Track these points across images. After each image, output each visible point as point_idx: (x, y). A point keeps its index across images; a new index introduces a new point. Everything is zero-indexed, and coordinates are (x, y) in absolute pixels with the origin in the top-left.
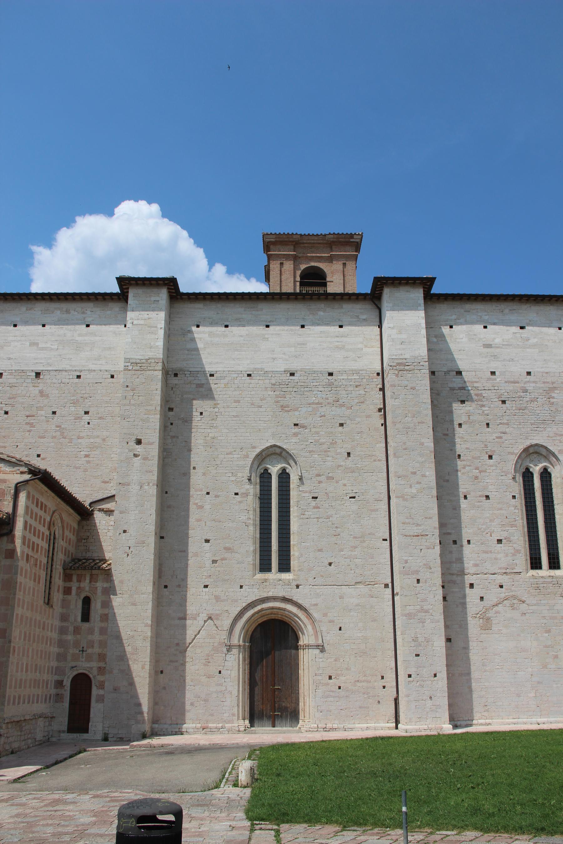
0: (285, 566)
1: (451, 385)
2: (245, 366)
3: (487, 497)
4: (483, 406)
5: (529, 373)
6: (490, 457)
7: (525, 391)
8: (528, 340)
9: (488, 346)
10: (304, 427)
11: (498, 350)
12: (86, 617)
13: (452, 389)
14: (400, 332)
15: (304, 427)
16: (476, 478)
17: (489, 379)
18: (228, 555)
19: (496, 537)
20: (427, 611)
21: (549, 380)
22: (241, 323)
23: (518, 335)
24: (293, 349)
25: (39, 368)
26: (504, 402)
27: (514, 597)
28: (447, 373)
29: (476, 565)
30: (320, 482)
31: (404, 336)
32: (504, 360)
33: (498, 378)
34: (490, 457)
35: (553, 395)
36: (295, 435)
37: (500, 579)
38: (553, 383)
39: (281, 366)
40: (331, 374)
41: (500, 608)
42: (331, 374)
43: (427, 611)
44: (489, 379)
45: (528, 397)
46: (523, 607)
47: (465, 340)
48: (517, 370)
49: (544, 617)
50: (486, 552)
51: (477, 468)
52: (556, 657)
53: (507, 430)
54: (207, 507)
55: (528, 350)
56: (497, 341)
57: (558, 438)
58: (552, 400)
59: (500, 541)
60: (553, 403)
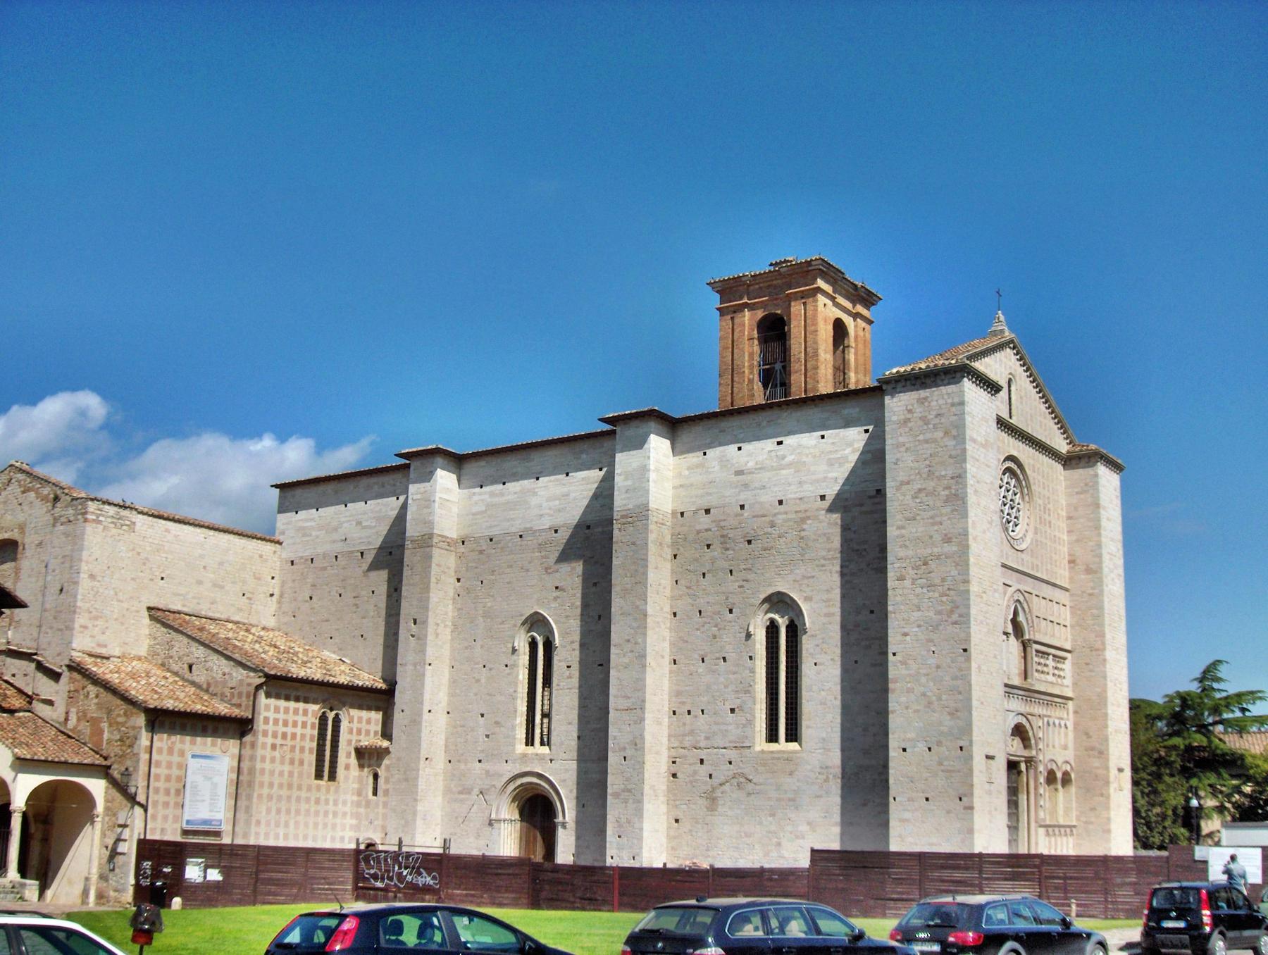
3: (724, 659)
4: (727, 549)
5: (780, 502)
6: (731, 611)
8: (784, 457)
9: (739, 473)
10: (563, 590)
11: (749, 477)
12: (375, 793)
14: (626, 479)
18: (497, 730)
20: (629, 791)
21: (803, 507)
22: (516, 477)
23: (773, 454)
24: (557, 502)
25: (363, 548)
26: (749, 542)
27: (742, 775)
28: (695, 512)
29: (707, 738)
31: (629, 483)
32: (756, 488)
33: (746, 513)
34: (731, 611)
35: (805, 526)
36: (555, 598)
37: (732, 754)
40: (588, 527)
41: (727, 787)
42: (588, 527)
43: (629, 791)
44: (736, 515)
45: (775, 532)
46: (750, 787)
47: (717, 468)
48: (769, 498)
49: (769, 799)
50: (716, 724)
51: (716, 626)
52: (779, 844)
53: (749, 577)
54: (483, 681)
55: (784, 472)
56: (751, 464)
57: (806, 581)
58: (803, 534)
59: (732, 710)
60: (802, 538)
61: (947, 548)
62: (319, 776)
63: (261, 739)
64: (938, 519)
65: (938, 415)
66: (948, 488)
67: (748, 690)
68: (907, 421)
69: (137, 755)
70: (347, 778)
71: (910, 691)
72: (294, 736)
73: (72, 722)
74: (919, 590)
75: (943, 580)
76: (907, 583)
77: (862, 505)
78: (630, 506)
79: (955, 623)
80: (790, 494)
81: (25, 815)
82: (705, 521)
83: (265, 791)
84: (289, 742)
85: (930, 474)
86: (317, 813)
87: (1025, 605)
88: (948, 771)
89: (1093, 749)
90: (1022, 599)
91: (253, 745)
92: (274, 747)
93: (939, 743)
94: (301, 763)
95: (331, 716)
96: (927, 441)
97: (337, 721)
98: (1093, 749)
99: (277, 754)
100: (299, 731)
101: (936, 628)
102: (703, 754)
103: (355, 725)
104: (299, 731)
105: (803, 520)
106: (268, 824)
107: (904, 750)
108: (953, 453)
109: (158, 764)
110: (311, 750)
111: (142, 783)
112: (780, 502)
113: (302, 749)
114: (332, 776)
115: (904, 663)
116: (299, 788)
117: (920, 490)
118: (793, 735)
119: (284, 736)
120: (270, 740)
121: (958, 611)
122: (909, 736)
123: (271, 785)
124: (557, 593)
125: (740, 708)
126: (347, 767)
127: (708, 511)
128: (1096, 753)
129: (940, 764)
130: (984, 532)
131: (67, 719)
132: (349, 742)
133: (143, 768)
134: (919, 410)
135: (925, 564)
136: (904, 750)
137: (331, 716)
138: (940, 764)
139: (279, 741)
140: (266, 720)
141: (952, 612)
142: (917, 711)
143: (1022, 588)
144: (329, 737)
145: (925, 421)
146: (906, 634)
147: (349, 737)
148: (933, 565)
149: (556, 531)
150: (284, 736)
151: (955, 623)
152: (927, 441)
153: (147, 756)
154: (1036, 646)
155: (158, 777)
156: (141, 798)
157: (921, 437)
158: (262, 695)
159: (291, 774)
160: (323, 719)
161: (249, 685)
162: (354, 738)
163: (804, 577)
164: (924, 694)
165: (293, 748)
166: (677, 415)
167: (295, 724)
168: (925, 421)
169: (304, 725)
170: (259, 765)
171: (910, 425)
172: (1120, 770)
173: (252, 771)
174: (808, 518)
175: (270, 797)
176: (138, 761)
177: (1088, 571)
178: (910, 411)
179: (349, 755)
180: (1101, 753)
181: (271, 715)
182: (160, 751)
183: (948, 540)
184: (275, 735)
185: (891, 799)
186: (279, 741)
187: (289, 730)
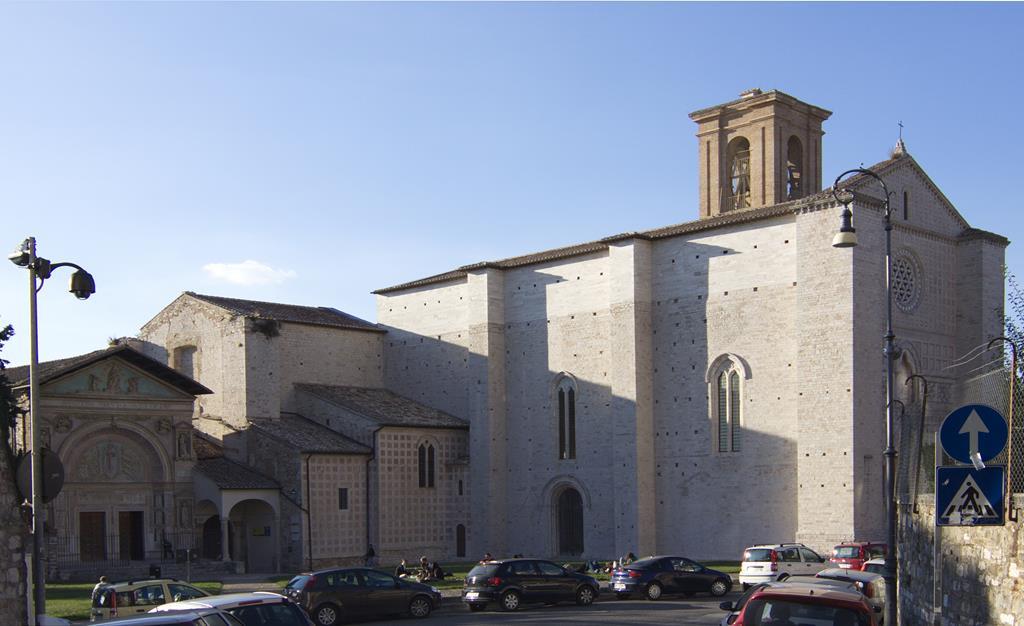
0: (572, 455)
1: (670, 312)
4: (690, 326)
5: (726, 293)
6: (694, 367)
8: (728, 262)
13: (671, 315)
15: (580, 356)
16: (683, 384)
17: (696, 303)
19: (693, 429)
28: (668, 302)
30: (589, 395)
34: (694, 367)
39: (566, 312)
42: (595, 314)
44: (696, 303)
47: (682, 271)
59: (696, 432)
61: (838, 323)
63: (380, 465)
64: (831, 304)
66: (840, 282)
68: (811, 236)
69: (300, 481)
72: (403, 461)
73: (252, 464)
74: (818, 352)
77: (783, 293)
78: (621, 301)
81: (229, 523)
83: (386, 497)
91: (376, 469)
92: (389, 469)
94: (409, 477)
95: (427, 447)
97: (431, 449)
99: (392, 473)
100: (406, 457)
104: (406, 457)
105: (744, 304)
108: (843, 258)
109: (314, 486)
110: (415, 469)
111: (304, 497)
112: (726, 293)
117: (821, 284)
119: (396, 461)
120: (386, 465)
121: (845, 365)
122: (813, 446)
123: (390, 493)
124: (575, 359)
125: (701, 429)
127: (676, 301)
130: (868, 310)
131: (248, 461)
133: (304, 489)
137: (427, 447)
140: (383, 453)
146: (810, 381)
147: (439, 458)
148: (828, 335)
149: (573, 317)
150: (396, 461)
151: (841, 373)
153: (306, 481)
155: (314, 494)
156: (305, 507)
157: (821, 248)
158: (379, 434)
159: (403, 484)
160: (422, 449)
161: (369, 431)
162: (444, 459)
163: (743, 343)
164: (821, 419)
169: (409, 453)
170: (380, 481)
171: (813, 239)
173: (377, 484)
174: (745, 304)
175: (390, 500)
176: (300, 485)
178: (814, 229)
182: (314, 477)
183: (838, 317)
184: (389, 462)
186: (392, 465)
187: (399, 457)
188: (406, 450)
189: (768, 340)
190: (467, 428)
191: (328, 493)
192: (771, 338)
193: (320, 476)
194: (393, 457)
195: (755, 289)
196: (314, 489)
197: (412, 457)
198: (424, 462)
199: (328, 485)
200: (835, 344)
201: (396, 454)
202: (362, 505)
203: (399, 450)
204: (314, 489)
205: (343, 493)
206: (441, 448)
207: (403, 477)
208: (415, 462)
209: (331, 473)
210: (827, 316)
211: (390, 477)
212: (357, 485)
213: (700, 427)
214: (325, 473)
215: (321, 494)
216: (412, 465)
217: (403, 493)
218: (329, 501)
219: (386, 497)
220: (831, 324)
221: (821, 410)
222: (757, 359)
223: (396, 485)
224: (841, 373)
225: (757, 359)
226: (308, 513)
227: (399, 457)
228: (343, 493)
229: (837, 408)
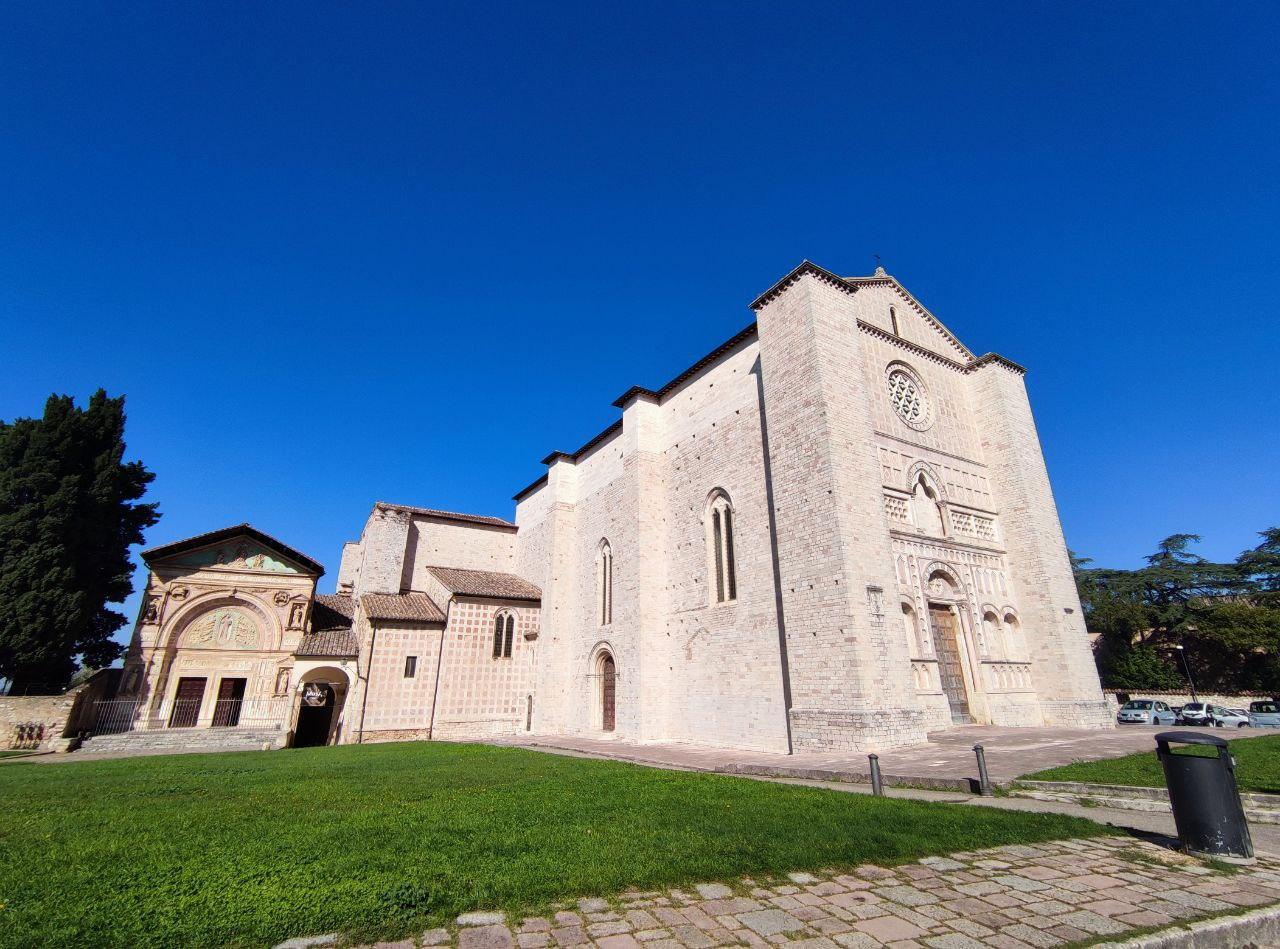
2: (596, 490)
7: (710, 442)
33: (696, 439)
38: (728, 425)
61: (808, 411)
62: (497, 653)
65: (792, 313)
67: (703, 564)
70: (518, 655)
71: (793, 538)
75: (808, 437)
76: (782, 449)
79: (819, 471)
80: (718, 418)
82: (676, 453)
83: (453, 665)
84: (472, 634)
85: (790, 360)
86: (494, 677)
87: (932, 473)
88: (830, 605)
89: (1034, 593)
90: (928, 469)
92: (460, 637)
93: (818, 580)
94: (482, 646)
95: (505, 618)
96: (786, 336)
97: (511, 620)
98: (1034, 593)
99: (463, 641)
101: (805, 481)
102: (682, 616)
103: (524, 622)
104: (480, 627)
105: (727, 433)
106: (455, 685)
107: (793, 590)
109: (378, 652)
110: (489, 638)
113: (483, 638)
114: (508, 654)
115: (786, 515)
116: (481, 662)
118: (733, 595)
119: (469, 630)
120: (457, 633)
121: (821, 460)
126: (518, 648)
128: (1037, 597)
129: (821, 599)
132: (520, 632)
134: (779, 316)
135: (794, 429)
136: (793, 590)
137: (505, 618)
138: (821, 599)
139: (464, 633)
141: (816, 462)
142: (798, 555)
143: (925, 459)
144: (505, 629)
145: (784, 320)
152: (786, 336)
154: (950, 507)
155: (377, 660)
158: (452, 603)
159: (474, 654)
160: (500, 620)
162: (524, 630)
164: (802, 539)
165: (475, 638)
166: (656, 390)
167: (477, 623)
168: (784, 320)
169: (484, 623)
172: (1069, 611)
177: (1000, 447)
178: (774, 319)
179: (519, 640)
180: (1042, 596)
181: (458, 618)
182: (380, 644)
183: (807, 404)
185: (787, 637)
186: (464, 633)
187: (472, 627)
188: (481, 619)
189: (751, 463)
190: (539, 601)
191: (394, 661)
192: (755, 459)
193: (388, 644)
194: (465, 626)
195: (737, 412)
196: (378, 657)
197: (487, 626)
198: (501, 631)
199: (395, 653)
200: (808, 437)
201: (469, 622)
202: (432, 674)
203: (474, 619)
204: (378, 657)
205: (411, 661)
206: (521, 619)
207: (474, 646)
208: (490, 631)
209: (401, 640)
210: (795, 407)
211: (459, 646)
212: (429, 654)
213: (699, 574)
214: (393, 640)
215: (385, 661)
216: (487, 634)
217: (473, 662)
218: (393, 669)
219: (453, 665)
220: (799, 416)
221: (801, 526)
222: (743, 486)
223: (466, 654)
224: (819, 471)
225: (743, 486)
226: (367, 681)
227: (472, 627)
228: (411, 661)
229: (819, 520)
